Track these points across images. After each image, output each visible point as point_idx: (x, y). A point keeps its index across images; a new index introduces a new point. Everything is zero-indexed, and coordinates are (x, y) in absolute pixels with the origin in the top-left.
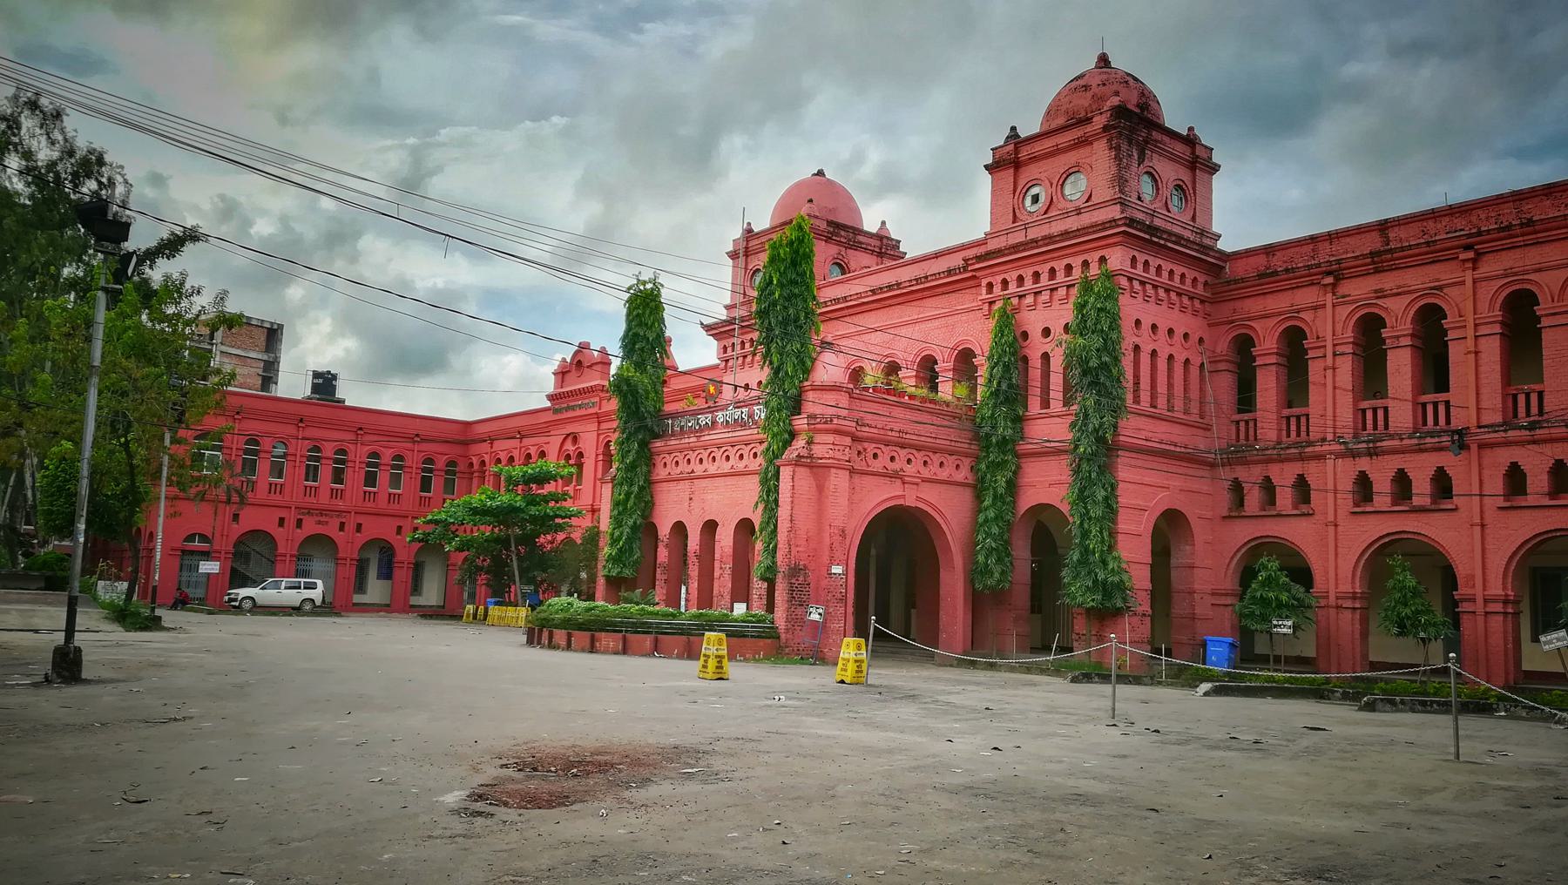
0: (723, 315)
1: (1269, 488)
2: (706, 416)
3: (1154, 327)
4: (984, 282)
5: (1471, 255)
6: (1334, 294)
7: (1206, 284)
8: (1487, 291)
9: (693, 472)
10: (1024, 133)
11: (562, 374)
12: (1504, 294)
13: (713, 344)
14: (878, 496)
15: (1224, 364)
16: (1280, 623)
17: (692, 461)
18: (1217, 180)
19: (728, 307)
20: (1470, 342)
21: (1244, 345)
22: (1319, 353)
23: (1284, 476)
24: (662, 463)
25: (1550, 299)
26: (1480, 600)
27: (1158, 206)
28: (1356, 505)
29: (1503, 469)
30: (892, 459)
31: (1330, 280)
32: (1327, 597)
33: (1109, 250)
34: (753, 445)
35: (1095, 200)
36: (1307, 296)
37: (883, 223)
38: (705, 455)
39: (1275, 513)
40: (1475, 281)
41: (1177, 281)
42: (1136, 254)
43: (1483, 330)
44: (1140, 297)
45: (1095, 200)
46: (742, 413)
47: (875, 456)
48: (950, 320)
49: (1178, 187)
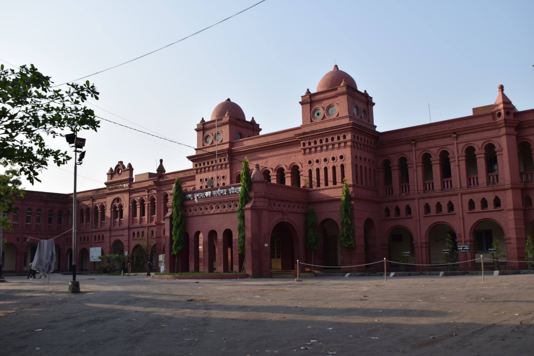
0: (194, 153)
1: (397, 209)
2: (208, 192)
3: (361, 158)
4: (302, 142)
5: (455, 135)
6: (415, 146)
7: (374, 143)
8: (461, 146)
9: (203, 213)
11: (112, 173)
12: (465, 148)
14: (277, 218)
16: (406, 253)
17: (203, 209)
18: (374, 107)
19: (196, 150)
20: (457, 162)
21: (387, 164)
22: (411, 166)
23: (402, 206)
24: (189, 210)
25: (478, 149)
26: (463, 242)
27: (359, 118)
28: (425, 214)
29: (468, 201)
30: (279, 206)
31: (414, 142)
32: (418, 244)
33: (347, 133)
34: (229, 203)
35: (340, 116)
36: (407, 147)
37: (253, 118)
38: (208, 207)
39: (400, 218)
40: (457, 144)
41: (369, 144)
42: (355, 134)
43: (460, 159)
44: (356, 148)
45: (340, 116)
46: (224, 191)
47: (274, 205)
48: (289, 155)
49: (364, 111)
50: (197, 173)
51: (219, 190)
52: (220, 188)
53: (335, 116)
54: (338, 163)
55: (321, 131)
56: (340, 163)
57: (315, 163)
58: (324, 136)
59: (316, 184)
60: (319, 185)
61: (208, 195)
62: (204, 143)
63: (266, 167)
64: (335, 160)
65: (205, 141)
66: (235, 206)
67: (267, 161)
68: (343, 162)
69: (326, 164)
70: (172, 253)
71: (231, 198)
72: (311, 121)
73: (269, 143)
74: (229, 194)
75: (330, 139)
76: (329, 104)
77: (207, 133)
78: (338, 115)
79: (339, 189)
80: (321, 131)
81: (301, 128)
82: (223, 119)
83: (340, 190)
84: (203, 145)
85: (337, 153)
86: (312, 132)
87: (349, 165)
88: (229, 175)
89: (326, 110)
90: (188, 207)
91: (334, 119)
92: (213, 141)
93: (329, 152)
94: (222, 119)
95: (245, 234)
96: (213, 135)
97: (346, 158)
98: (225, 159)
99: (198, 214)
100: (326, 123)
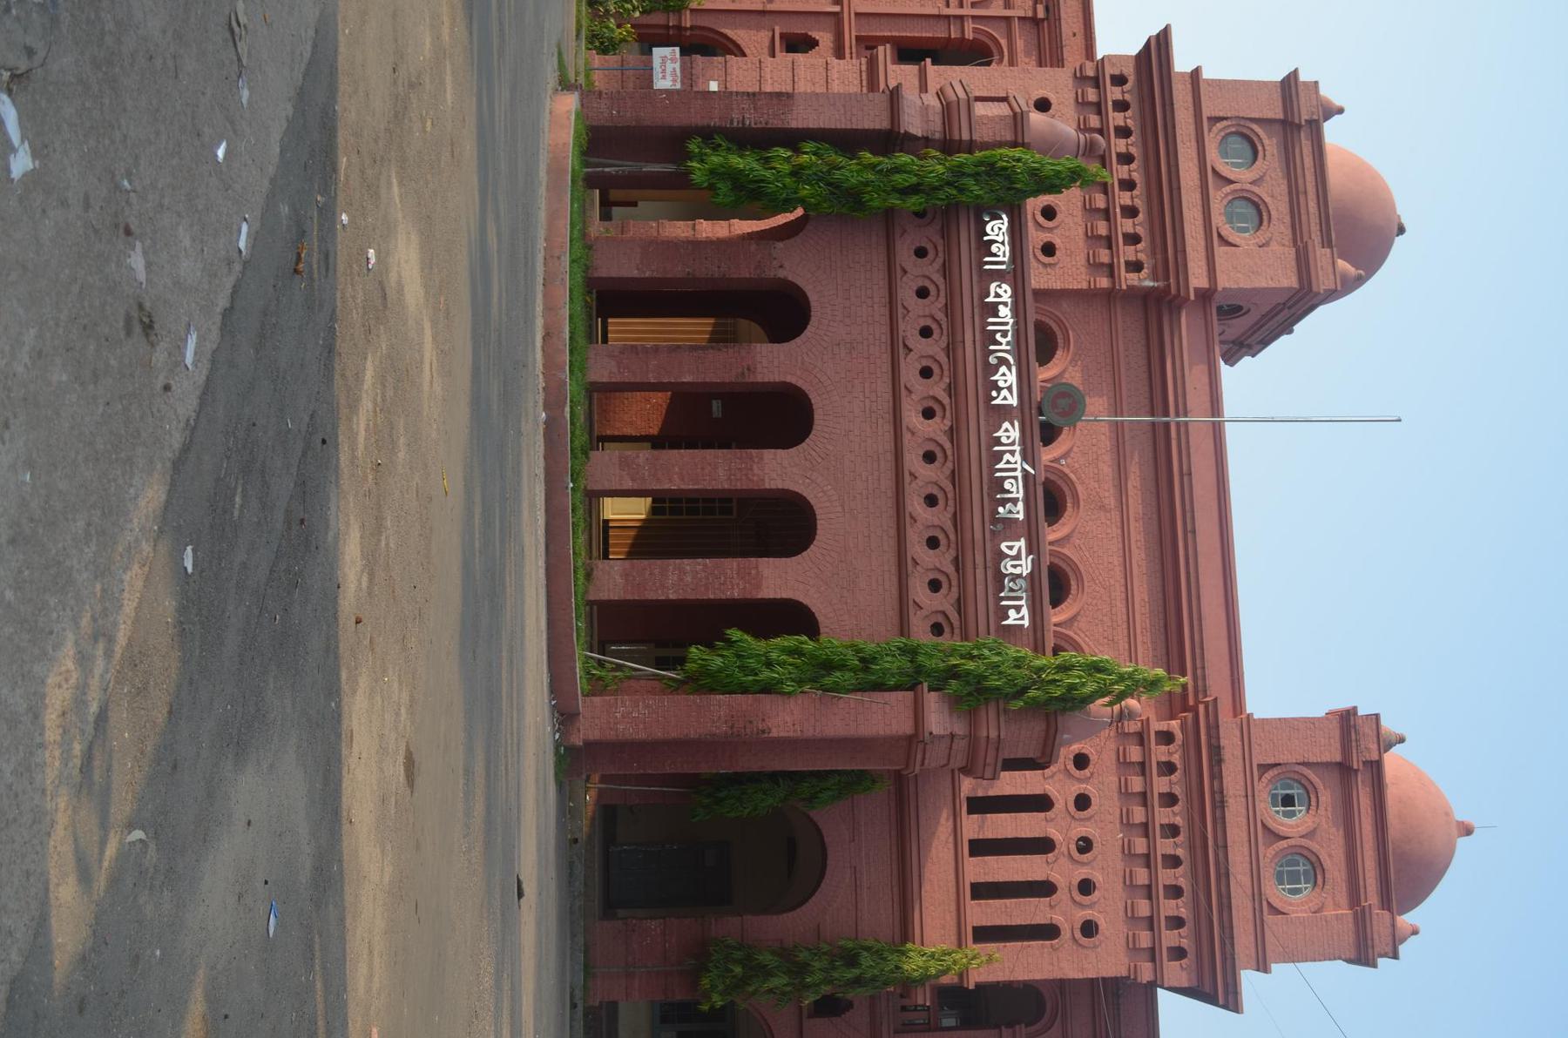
0: (1182, 63)
4: (1175, 725)
10: (1390, 759)
13: (1132, 46)
15: (997, 734)
19: (1196, 74)
24: (925, 244)
34: (952, 537)
35: (1269, 919)
45: (1269, 919)
46: (1015, 501)
50: (1080, 78)
51: (1027, 467)
52: (1033, 472)
53: (1276, 893)
54: (1062, 911)
55: (1220, 843)
57: (1076, 789)
58: (1191, 848)
59: (980, 794)
60: (980, 805)
61: (1001, 384)
62: (1225, 123)
64: (1078, 897)
65: (1233, 130)
66: (932, 576)
67: (1102, 508)
68: (1068, 935)
69: (1066, 853)
70: (693, 146)
71: (980, 571)
72: (1264, 768)
74: (997, 537)
75: (1176, 878)
76: (1327, 863)
77: (1270, 144)
78: (1275, 911)
79: (954, 914)
80: (1220, 843)
81: (1235, 716)
82: (1328, 250)
83: (948, 918)
84: (1215, 120)
85: (1107, 908)
86: (1217, 797)
87: (1051, 968)
88: (1058, 286)
89: (1301, 846)
90: (945, 233)
91: (1257, 895)
92: (1231, 182)
93: (1120, 865)
94: (1330, 246)
96: (1253, 183)
97: (1085, 951)
98: (1136, 267)
100: (1246, 850)
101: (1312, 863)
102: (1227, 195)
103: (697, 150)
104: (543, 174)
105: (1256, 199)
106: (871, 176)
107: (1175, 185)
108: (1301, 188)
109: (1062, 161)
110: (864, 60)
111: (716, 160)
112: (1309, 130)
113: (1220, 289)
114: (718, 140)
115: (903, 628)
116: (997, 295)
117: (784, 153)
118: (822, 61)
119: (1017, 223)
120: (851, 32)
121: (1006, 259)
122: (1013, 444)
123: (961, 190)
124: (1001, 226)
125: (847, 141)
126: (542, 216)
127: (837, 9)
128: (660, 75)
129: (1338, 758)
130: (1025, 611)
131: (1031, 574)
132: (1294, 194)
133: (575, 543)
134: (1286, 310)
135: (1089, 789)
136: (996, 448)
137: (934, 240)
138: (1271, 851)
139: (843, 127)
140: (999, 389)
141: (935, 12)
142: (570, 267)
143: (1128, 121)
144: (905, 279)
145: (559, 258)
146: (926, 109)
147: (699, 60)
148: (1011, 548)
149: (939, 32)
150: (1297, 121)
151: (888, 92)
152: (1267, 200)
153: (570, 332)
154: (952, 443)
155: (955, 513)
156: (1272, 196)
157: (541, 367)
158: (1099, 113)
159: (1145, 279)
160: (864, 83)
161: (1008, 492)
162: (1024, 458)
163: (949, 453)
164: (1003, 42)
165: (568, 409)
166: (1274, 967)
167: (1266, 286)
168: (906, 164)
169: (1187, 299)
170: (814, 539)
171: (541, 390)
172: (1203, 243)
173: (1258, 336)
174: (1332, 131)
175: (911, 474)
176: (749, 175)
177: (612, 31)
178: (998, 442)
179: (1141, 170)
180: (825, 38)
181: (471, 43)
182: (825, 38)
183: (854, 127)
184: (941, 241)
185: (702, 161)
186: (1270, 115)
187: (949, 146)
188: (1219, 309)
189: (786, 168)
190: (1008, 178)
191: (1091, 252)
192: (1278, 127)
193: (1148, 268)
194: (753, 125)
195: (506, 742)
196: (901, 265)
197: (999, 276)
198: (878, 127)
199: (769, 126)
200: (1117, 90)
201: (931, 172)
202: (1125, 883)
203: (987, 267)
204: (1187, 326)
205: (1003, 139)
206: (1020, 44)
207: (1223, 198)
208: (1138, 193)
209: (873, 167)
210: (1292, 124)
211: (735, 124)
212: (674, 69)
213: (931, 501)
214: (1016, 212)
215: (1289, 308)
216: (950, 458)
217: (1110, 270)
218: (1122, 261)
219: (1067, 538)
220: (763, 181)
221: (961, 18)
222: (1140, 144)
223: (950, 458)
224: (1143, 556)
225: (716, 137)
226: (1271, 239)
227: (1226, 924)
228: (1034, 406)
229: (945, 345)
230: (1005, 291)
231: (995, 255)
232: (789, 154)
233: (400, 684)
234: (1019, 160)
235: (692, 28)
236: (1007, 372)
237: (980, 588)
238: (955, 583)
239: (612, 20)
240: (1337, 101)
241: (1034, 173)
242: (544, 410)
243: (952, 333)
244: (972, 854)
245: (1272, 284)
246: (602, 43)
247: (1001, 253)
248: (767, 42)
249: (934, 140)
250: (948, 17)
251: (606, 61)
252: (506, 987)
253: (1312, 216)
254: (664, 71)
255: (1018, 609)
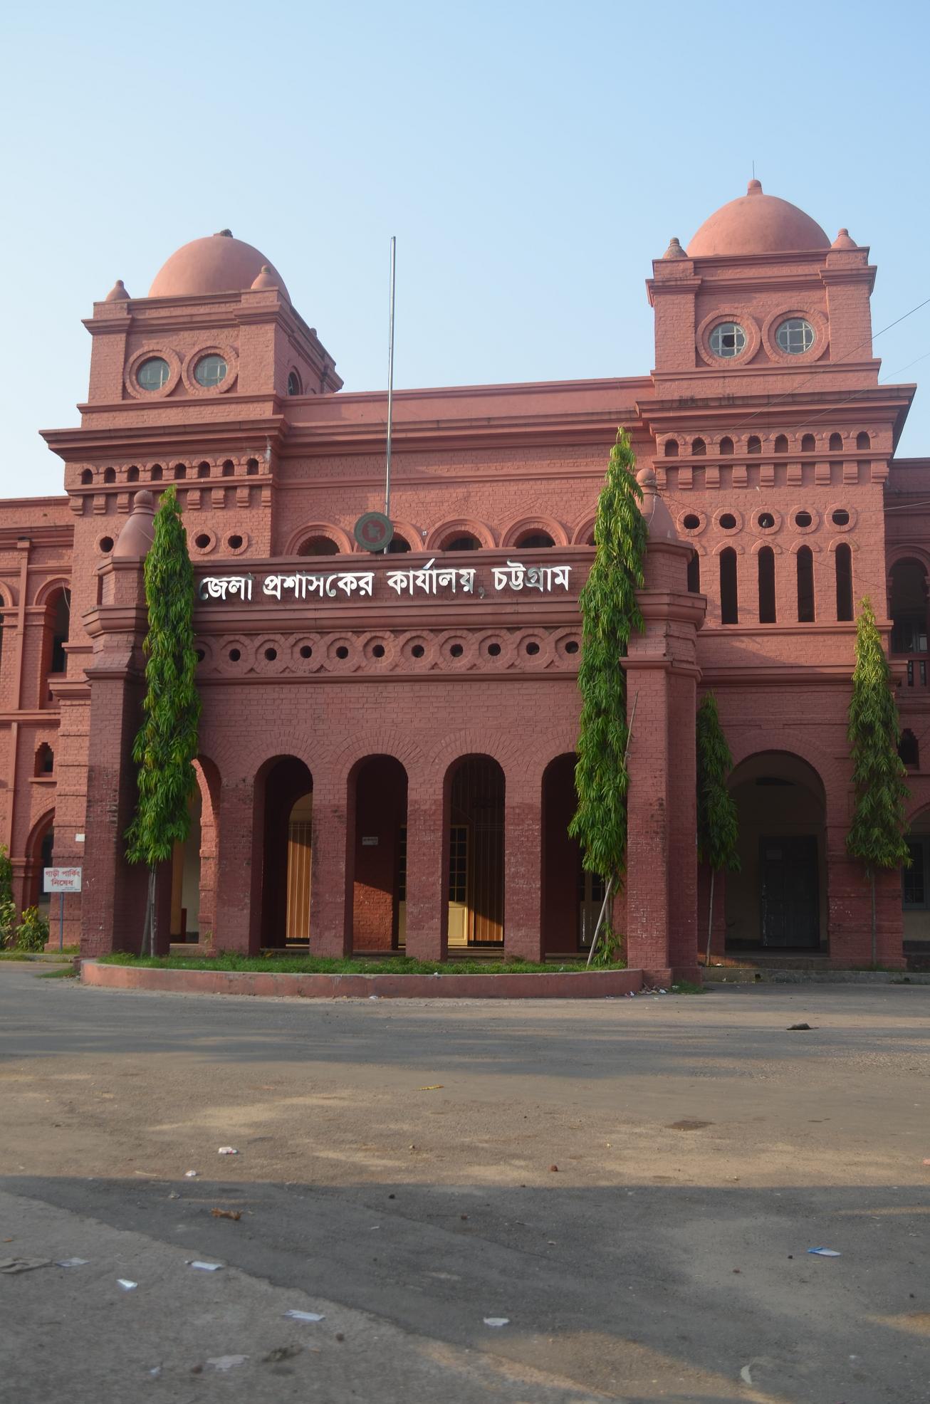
0: (74, 421)
4: (660, 439)
13: (57, 465)
15: (666, 597)
19: (83, 409)
24: (227, 652)
34: (489, 633)
35: (833, 359)
45: (833, 359)
46: (459, 576)
50: (84, 511)
51: (428, 565)
52: (433, 560)
53: (810, 353)
54: (825, 543)
55: (765, 401)
56: (832, 538)
57: (716, 527)
58: (770, 426)
59: (719, 612)
61: (354, 586)
62: (128, 384)
63: (461, 522)
64: (813, 527)
65: (134, 377)
66: (524, 651)
68: (846, 536)
69: (773, 537)
70: (134, 857)
71: (521, 609)
72: (699, 361)
73: (493, 423)
74: (491, 592)
77: (148, 345)
78: (826, 354)
79: (826, 637)
80: (765, 401)
81: (652, 386)
82: (243, 297)
83: (830, 642)
85: (822, 502)
87: (875, 552)
88: (268, 534)
89: (769, 330)
90: (219, 634)
91: (812, 369)
93: (784, 490)
94: (239, 295)
95: (627, 781)
96: (182, 361)
98: (253, 466)
99: (359, 673)
100: (771, 379)
101: (784, 321)
102: (191, 384)
103: (138, 854)
104: (156, 994)
105: (196, 359)
106: (165, 699)
107: (183, 430)
108: (186, 319)
109: (156, 529)
110: (62, 703)
111: (146, 837)
112: (137, 311)
113: (274, 392)
114: (129, 835)
115: (570, 678)
116: (275, 588)
117: (142, 776)
118: (61, 740)
119: (208, 570)
120: (36, 714)
121: (243, 580)
122: (407, 577)
123: (180, 618)
124: (213, 584)
125: (134, 719)
126: (193, 995)
127: (15, 726)
128: (69, 885)
129: (691, 297)
130: (557, 570)
131: (524, 563)
132: (192, 325)
133: (488, 971)
134: (295, 334)
135: (716, 515)
136: (411, 592)
137: (224, 644)
138: (774, 357)
139: (120, 722)
140: (359, 588)
141: (20, 638)
142: (239, 971)
143: (123, 469)
144: (258, 670)
145: (231, 981)
146: (107, 647)
147: (56, 850)
148: (500, 581)
149: (39, 635)
150: (128, 322)
151: (91, 681)
152: (197, 349)
153: (298, 972)
154: (405, 631)
155: (469, 630)
156: (194, 345)
157: (329, 999)
158: (115, 495)
159: (264, 457)
160: (82, 702)
161: (450, 582)
162: (420, 567)
163: (414, 634)
164: (50, 578)
165: (367, 976)
166: (875, 356)
167: (273, 352)
168: (155, 667)
169: (283, 420)
170: (489, 756)
171: (349, 1000)
172: (233, 406)
173: (317, 360)
174: (139, 290)
175: (433, 668)
176: (161, 808)
177: (27, 928)
178: (405, 590)
179: (168, 458)
180: (41, 737)
181: (35, 1056)
182: (41, 737)
183: (121, 712)
184: (225, 637)
185: (147, 850)
186: (122, 346)
187: (141, 629)
188: (292, 393)
189: (156, 774)
190: (171, 576)
191: (239, 504)
192: (134, 338)
193: (254, 455)
194: (117, 803)
195: (668, 1037)
196: (246, 674)
197: (258, 587)
198: (121, 691)
199: (118, 788)
200: (95, 478)
201: (163, 644)
202: (800, 486)
203: (250, 597)
204: (304, 421)
205: (136, 580)
206: (52, 563)
207: (194, 388)
208: (188, 462)
209: (157, 696)
210: (131, 326)
211: (115, 819)
212: (64, 873)
213: (457, 651)
214: (203, 570)
215: (293, 331)
216: (418, 633)
217: (256, 488)
218: (247, 477)
219: (492, 530)
220: (167, 796)
221: (27, 615)
222: (145, 459)
223: (418, 633)
224: (509, 464)
225: (126, 836)
226: (231, 347)
227: (836, 397)
228: (374, 558)
229: (318, 636)
230: (272, 581)
231: (239, 589)
232: (143, 771)
233: (611, 1132)
234: (155, 567)
235: (27, 856)
236: (344, 581)
237: (535, 608)
238: (530, 631)
239: (18, 928)
240: (112, 286)
241: (167, 554)
242: (368, 997)
243: (308, 629)
244: (773, 620)
245: (272, 346)
246: (38, 938)
247: (238, 585)
248: (43, 789)
249: (135, 643)
250: (25, 627)
251: (54, 935)
252: (889, 1041)
253: (213, 311)
254: (65, 882)
255: (555, 575)
